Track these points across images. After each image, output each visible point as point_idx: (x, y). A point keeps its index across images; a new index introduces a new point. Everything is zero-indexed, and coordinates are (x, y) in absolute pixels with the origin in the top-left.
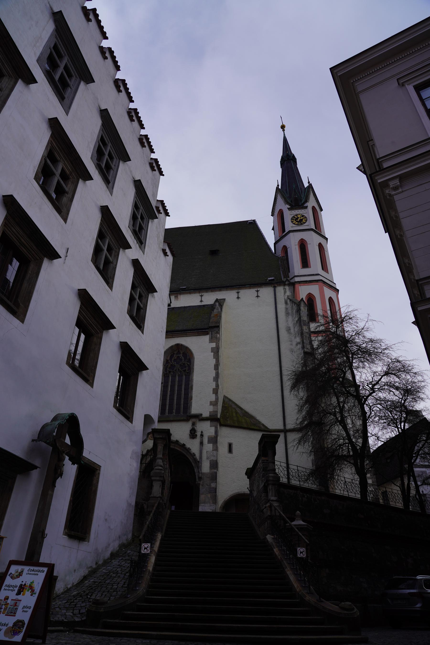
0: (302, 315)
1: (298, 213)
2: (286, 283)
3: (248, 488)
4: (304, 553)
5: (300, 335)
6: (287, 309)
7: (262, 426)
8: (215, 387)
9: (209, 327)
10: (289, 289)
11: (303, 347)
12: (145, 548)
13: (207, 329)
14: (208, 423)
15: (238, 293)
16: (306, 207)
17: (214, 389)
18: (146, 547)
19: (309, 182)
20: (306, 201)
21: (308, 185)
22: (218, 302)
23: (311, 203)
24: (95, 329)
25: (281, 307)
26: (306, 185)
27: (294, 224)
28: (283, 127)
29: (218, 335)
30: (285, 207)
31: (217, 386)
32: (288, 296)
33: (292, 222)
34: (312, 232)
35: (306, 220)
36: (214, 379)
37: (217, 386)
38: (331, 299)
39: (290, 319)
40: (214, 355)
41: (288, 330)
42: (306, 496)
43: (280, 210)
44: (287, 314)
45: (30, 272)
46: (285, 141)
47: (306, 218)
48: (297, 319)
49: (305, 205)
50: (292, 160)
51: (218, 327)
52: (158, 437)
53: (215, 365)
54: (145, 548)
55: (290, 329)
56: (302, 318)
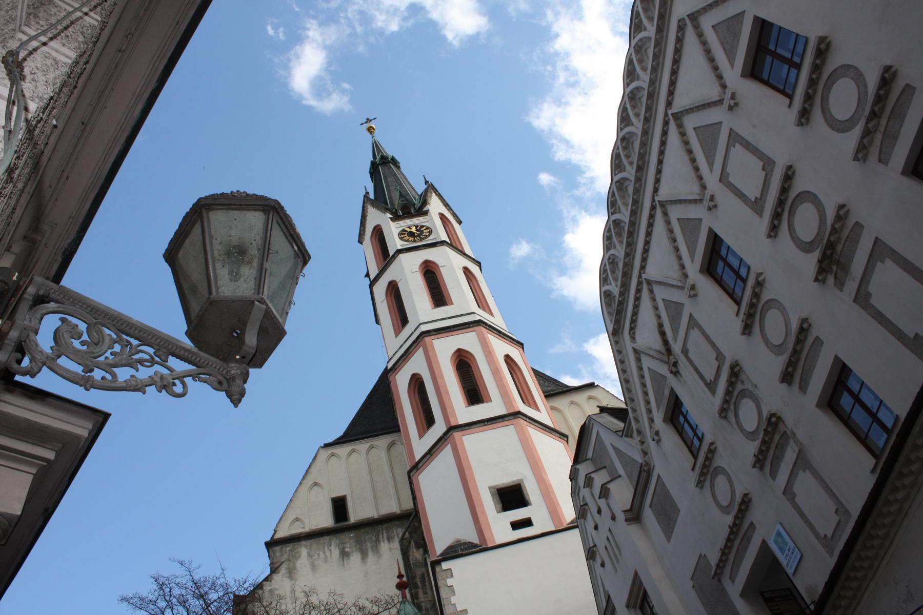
16: (426, 213)
19: (426, 182)
23: (435, 206)
27: (407, 241)
28: (370, 130)
33: (402, 239)
34: (446, 249)
35: (431, 232)
46: (376, 146)
47: (428, 228)
49: (425, 209)
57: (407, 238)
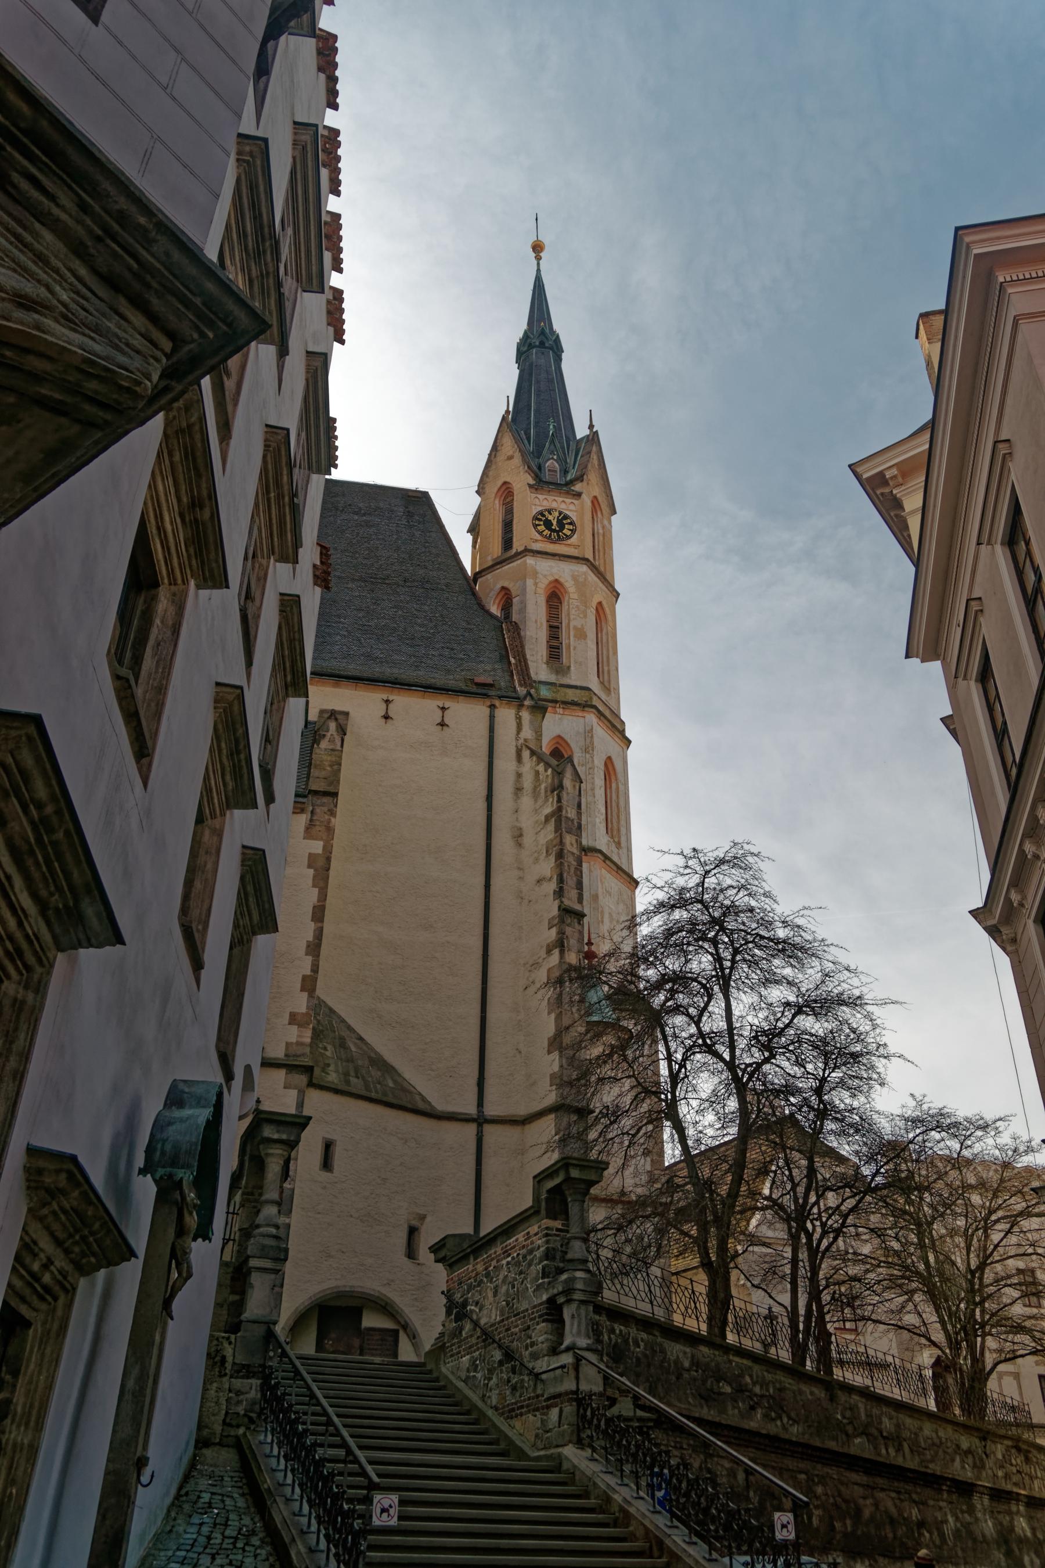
0: (564, 802)
1: (554, 505)
2: (527, 702)
3: (443, 1293)
4: (790, 1527)
5: (552, 858)
6: (519, 775)
7: (418, 1098)
8: (308, 972)
9: (310, 791)
10: (531, 722)
11: (559, 893)
12: (383, 1510)
13: (305, 796)
14: (281, 1074)
15: (387, 702)
16: (578, 495)
17: (305, 978)
18: (386, 1506)
19: (591, 427)
20: (580, 478)
21: (588, 432)
22: (336, 719)
24: (213, 805)
25: (506, 765)
26: (581, 431)
27: (540, 533)
28: (538, 248)
29: (333, 820)
30: (521, 480)
31: (315, 969)
32: (526, 740)
33: (535, 526)
35: (573, 531)
36: (308, 946)
37: (315, 969)
38: (609, 762)
39: (526, 801)
40: (315, 877)
41: (518, 836)
42: (618, 1332)
43: (505, 483)
44: (518, 790)
45: (158, 621)
48: (548, 810)
49: (578, 487)
50: (551, 348)
51: (335, 795)
52: (276, 1136)
53: (314, 907)
54: (384, 1510)
55: (521, 835)
56: (564, 812)
57: (542, 528)
